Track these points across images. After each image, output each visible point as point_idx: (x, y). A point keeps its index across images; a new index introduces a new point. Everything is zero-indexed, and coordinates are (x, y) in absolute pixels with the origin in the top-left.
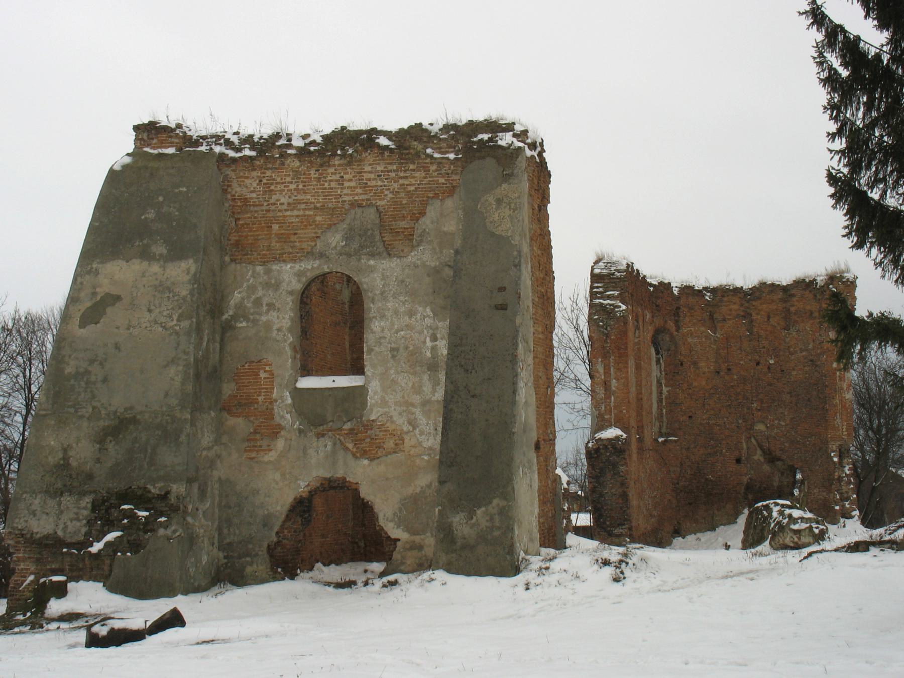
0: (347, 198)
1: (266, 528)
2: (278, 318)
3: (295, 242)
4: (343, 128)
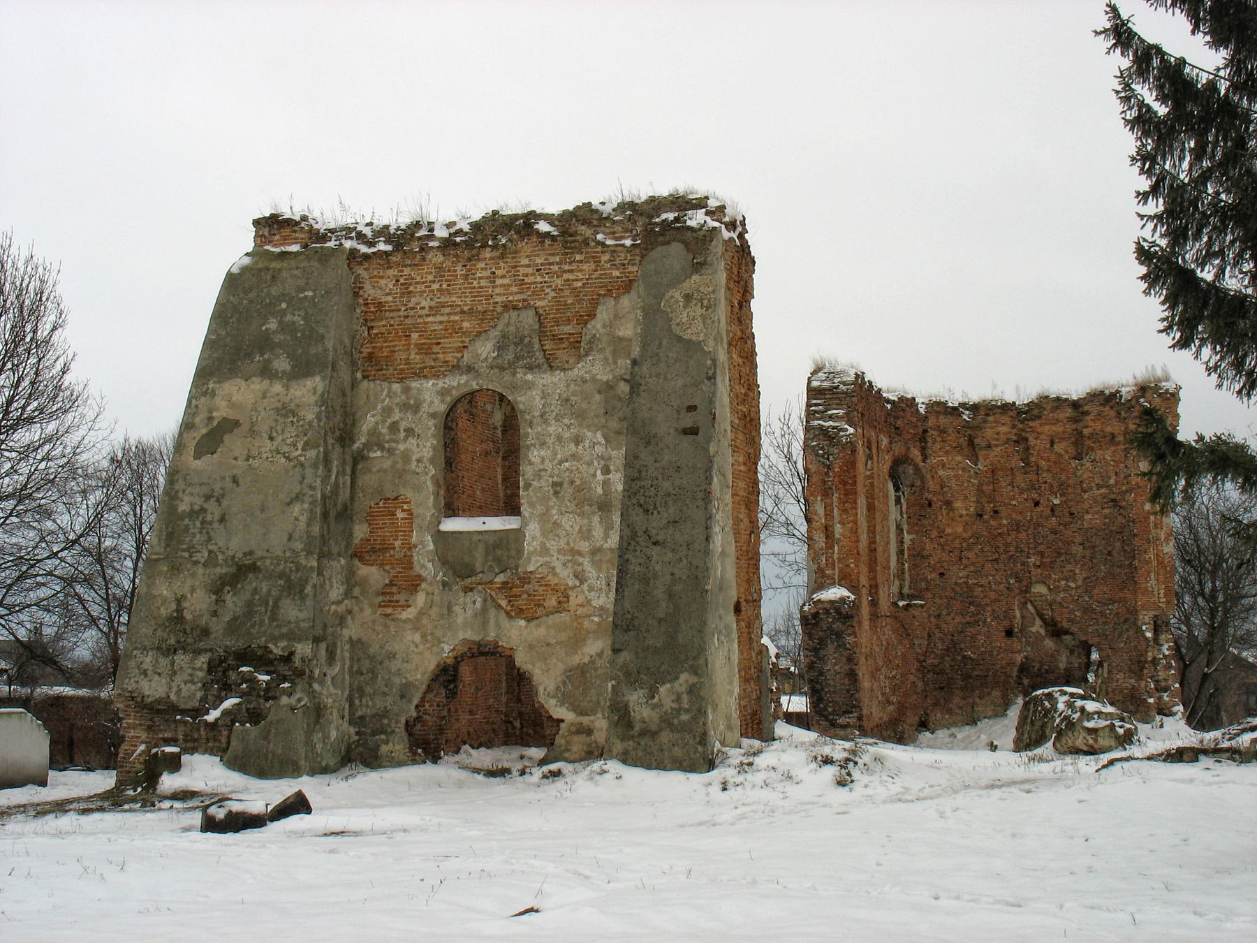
0: (499, 299)
1: (404, 700)
2: (418, 445)
3: (438, 353)
4: (495, 213)
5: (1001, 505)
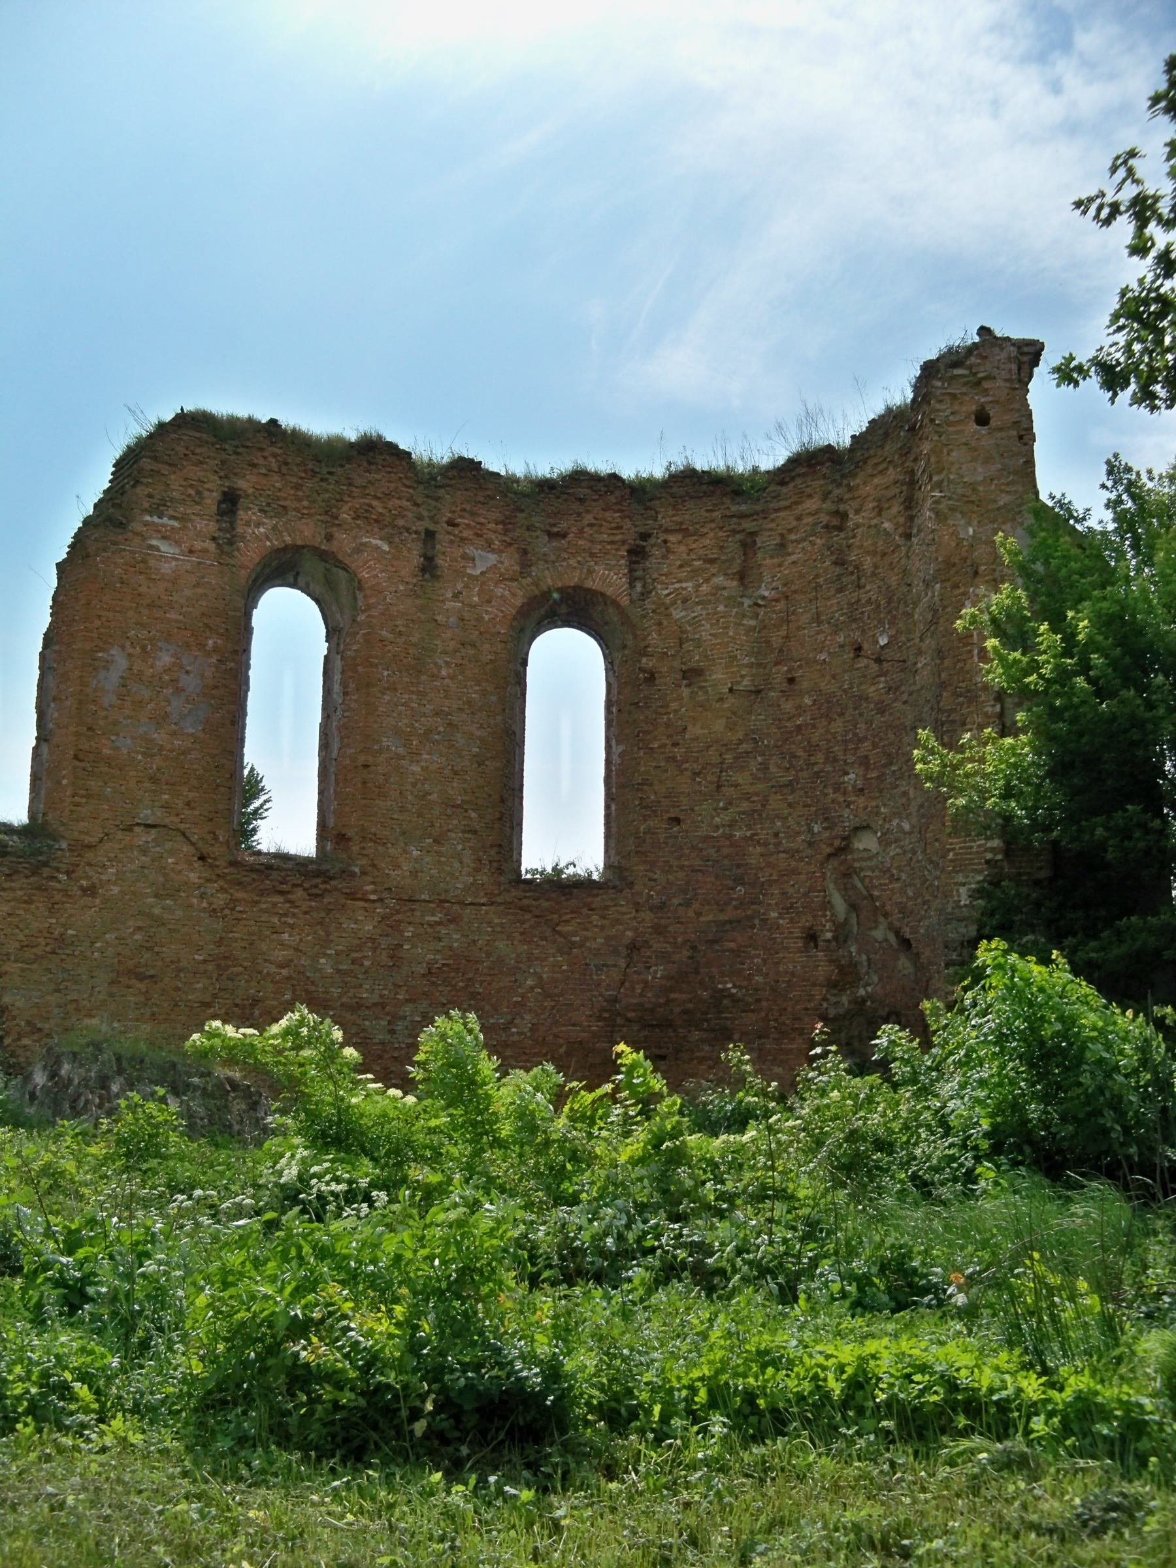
5: (800, 667)
